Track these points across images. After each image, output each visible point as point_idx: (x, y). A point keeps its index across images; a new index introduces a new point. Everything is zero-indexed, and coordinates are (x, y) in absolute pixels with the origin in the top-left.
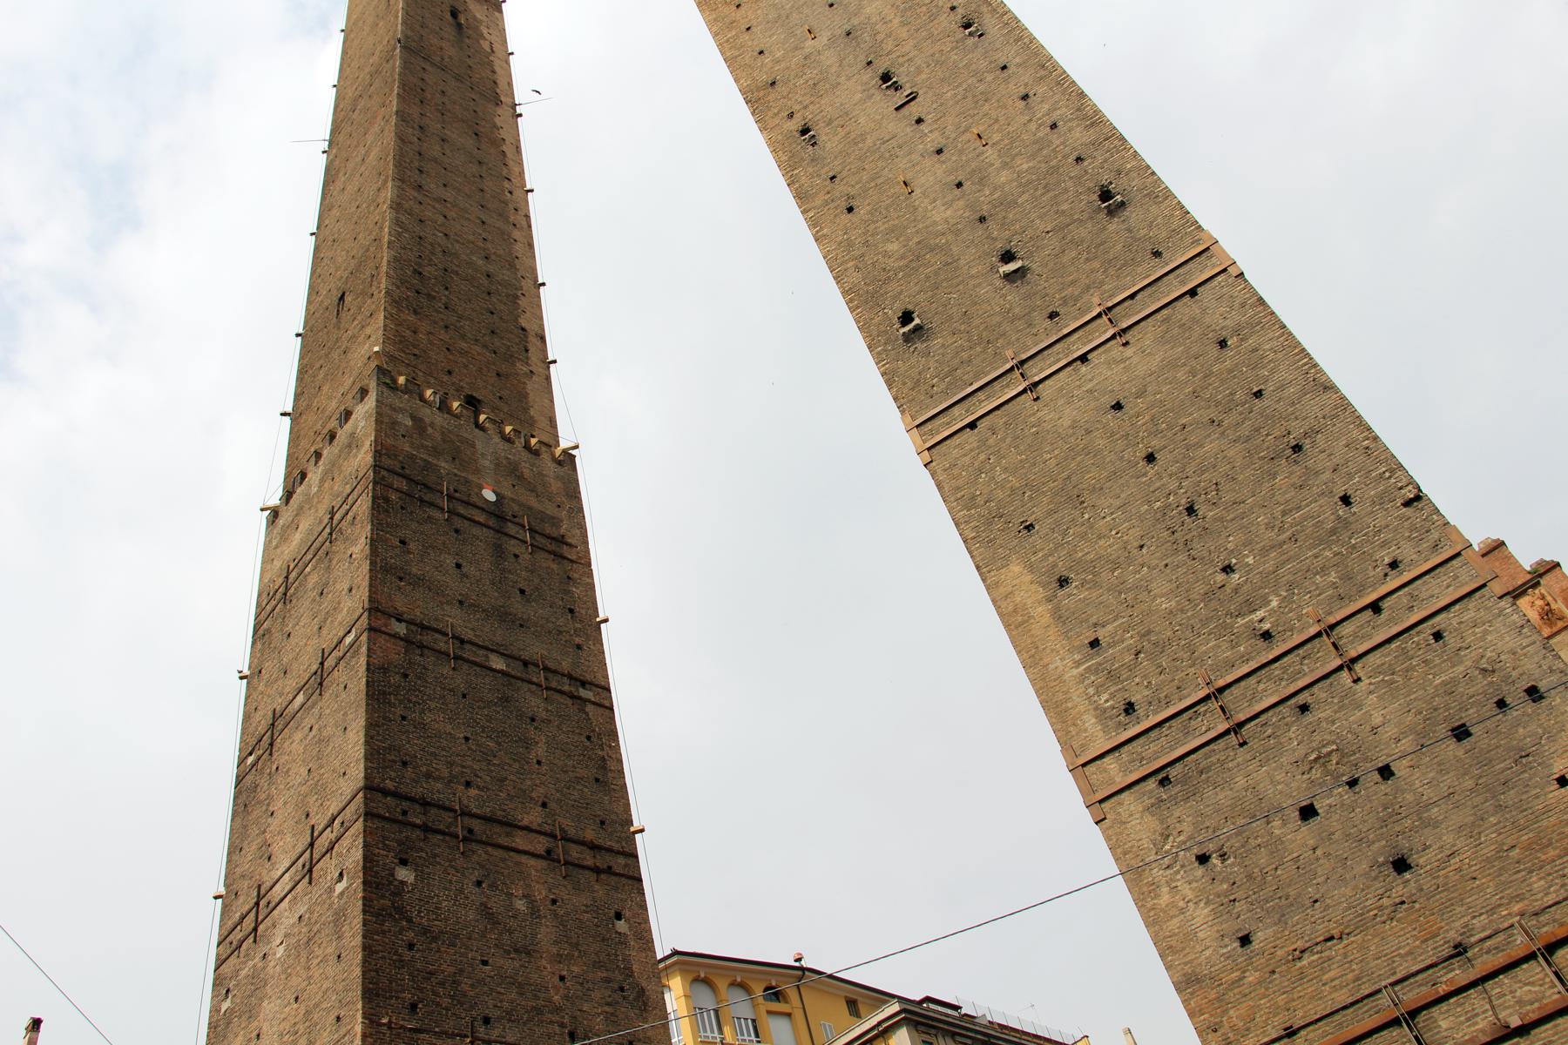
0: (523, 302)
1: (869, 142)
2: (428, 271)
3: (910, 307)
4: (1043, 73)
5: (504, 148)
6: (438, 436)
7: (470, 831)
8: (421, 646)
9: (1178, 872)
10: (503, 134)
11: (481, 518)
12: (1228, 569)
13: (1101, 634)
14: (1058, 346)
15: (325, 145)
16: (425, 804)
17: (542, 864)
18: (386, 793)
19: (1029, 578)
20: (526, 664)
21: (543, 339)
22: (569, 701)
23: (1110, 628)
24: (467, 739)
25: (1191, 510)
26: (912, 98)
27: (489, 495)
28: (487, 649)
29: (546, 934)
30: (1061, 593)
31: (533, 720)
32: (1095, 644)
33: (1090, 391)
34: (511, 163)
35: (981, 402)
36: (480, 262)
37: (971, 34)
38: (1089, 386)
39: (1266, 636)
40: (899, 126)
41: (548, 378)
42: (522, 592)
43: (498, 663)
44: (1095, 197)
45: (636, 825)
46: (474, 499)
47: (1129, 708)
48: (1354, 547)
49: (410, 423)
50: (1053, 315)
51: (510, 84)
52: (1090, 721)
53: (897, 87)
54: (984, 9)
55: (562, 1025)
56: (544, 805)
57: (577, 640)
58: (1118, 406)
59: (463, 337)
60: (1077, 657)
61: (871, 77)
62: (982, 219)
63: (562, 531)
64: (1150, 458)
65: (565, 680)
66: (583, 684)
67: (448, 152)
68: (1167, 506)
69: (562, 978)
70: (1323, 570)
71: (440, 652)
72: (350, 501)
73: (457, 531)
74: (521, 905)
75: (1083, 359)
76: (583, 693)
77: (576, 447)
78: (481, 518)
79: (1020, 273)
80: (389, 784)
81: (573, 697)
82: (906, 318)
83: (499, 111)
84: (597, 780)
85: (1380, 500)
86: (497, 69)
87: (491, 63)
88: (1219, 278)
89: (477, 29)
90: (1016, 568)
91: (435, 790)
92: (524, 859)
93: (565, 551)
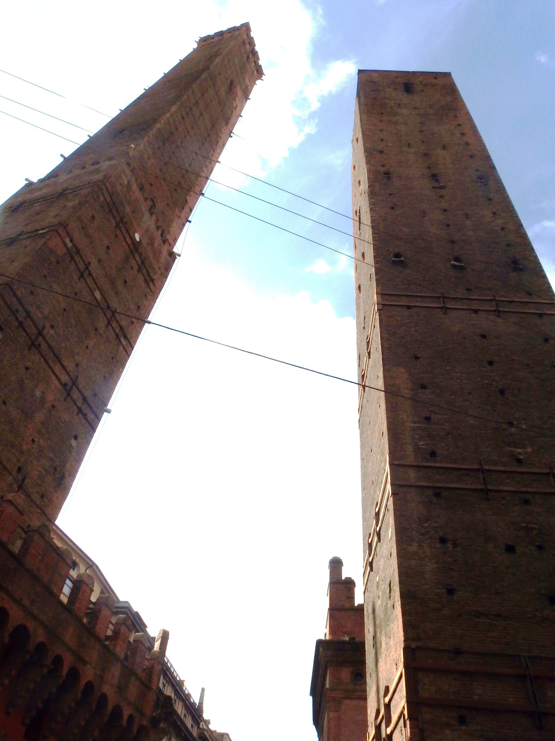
1: (414, 191)
3: (402, 253)
6: (133, 198)
7: (39, 345)
8: (72, 258)
9: (427, 539)
11: (129, 242)
12: (511, 424)
13: (434, 417)
15: (147, 88)
16: (28, 315)
17: (59, 386)
18: (15, 295)
19: (407, 376)
20: (108, 307)
21: (191, 210)
22: (115, 337)
23: (439, 417)
24: (65, 310)
25: (502, 392)
26: (443, 187)
27: (137, 237)
28: (97, 286)
29: (40, 416)
30: (420, 390)
31: (96, 330)
32: (428, 419)
34: (218, 147)
35: (417, 301)
37: (480, 182)
38: (474, 322)
39: (519, 461)
41: (184, 225)
42: (125, 282)
43: (98, 295)
45: (109, 407)
46: (131, 233)
47: (433, 454)
49: (126, 183)
50: (468, 290)
51: (234, 124)
52: (409, 449)
53: (437, 181)
54: (492, 178)
55: (18, 461)
56: (77, 365)
58: (483, 336)
60: (416, 419)
62: (453, 242)
63: (154, 277)
65: (119, 328)
66: (125, 337)
69: (33, 441)
71: (78, 268)
72: (79, 188)
73: (116, 236)
74: (38, 393)
75: (476, 311)
76: (122, 339)
77: (179, 255)
79: (461, 268)
80: (19, 293)
81: (117, 335)
82: (397, 255)
83: (226, 128)
87: (232, 112)
91: (37, 315)
92: (54, 377)
93: (151, 285)
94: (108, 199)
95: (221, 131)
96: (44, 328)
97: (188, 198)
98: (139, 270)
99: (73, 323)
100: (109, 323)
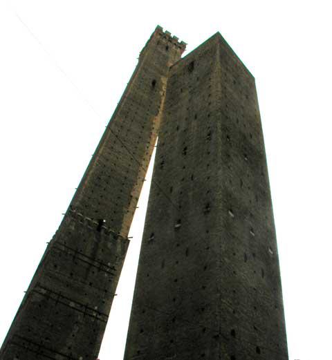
0: (135, 187)
2: (102, 177)
11: (86, 259)
16: (30, 341)
20: (82, 306)
34: (152, 136)
36: (125, 173)
41: (133, 213)
43: (72, 304)
57: (104, 300)
76: (98, 317)
78: (86, 259)
83: (156, 117)
84: (91, 343)
89: (162, 87)
93: (113, 272)
94: (63, 248)
95: (152, 124)
96: (42, 342)
97: (132, 194)
98: (99, 269)
99: (60, 328)
100: (85, 314)
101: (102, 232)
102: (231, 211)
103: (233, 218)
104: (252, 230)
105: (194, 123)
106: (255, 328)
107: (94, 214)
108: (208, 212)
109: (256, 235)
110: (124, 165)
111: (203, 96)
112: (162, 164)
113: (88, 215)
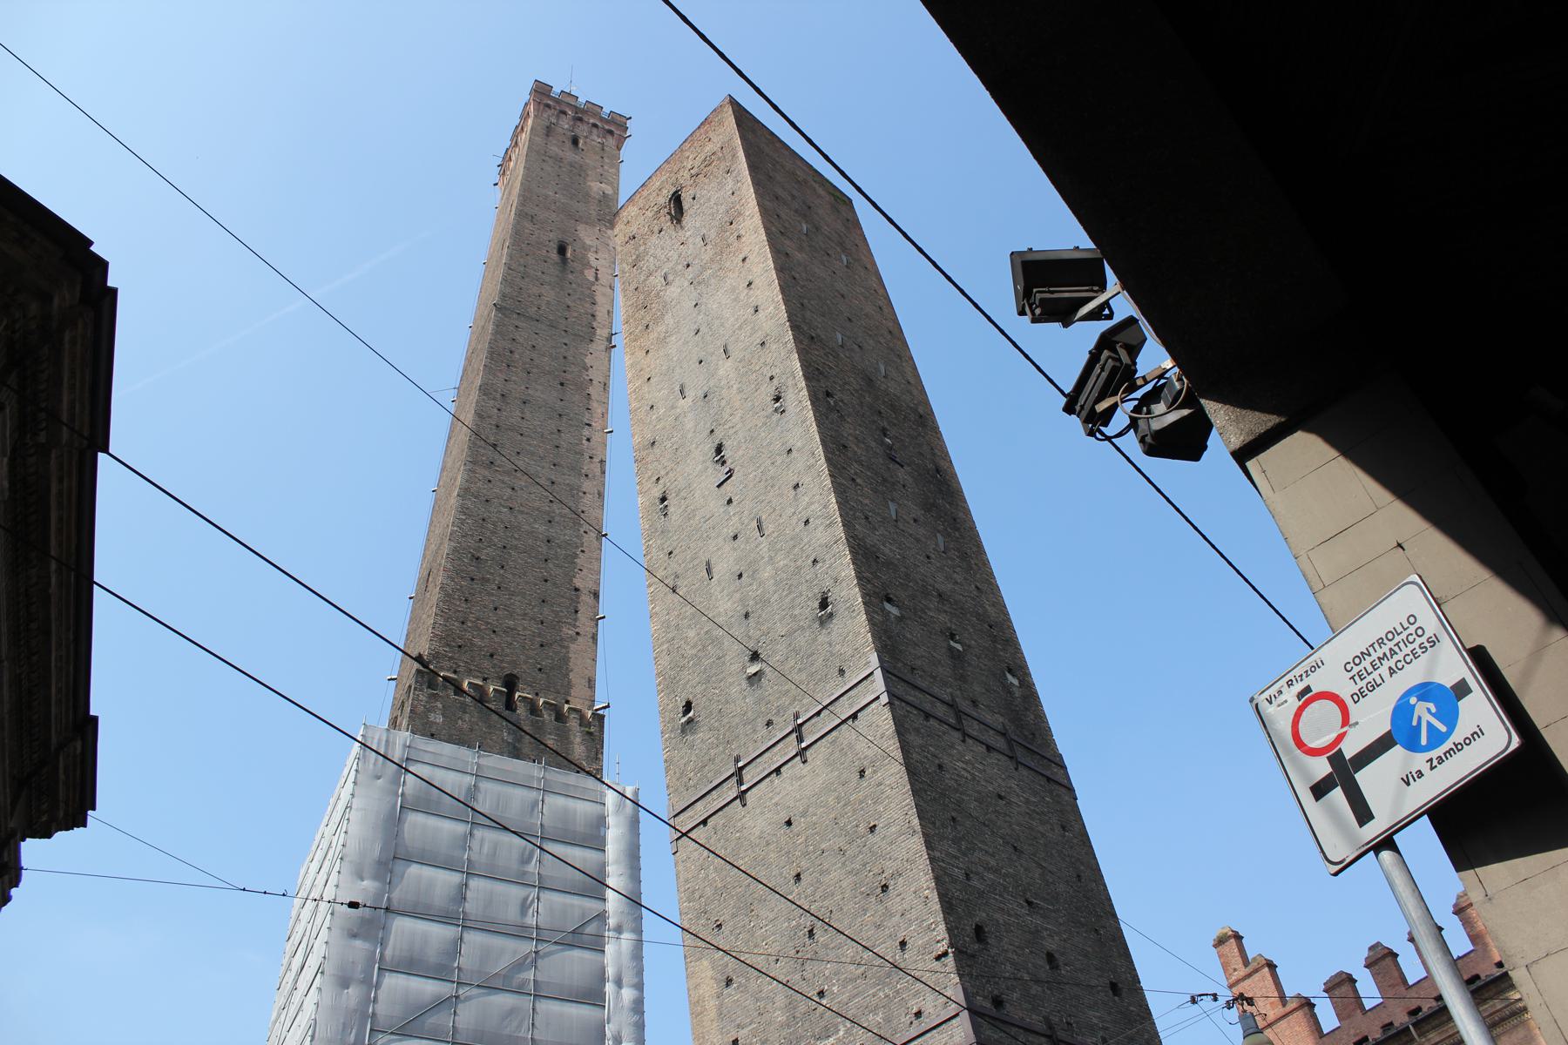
4: (812, 461)
5: (591, 390)
10: (592, 374)
14: (766, 755)
23: (746, 1031)
33: (776, 804)
34: (594, 405)
40: (715, 505)
41: (594, 638)
44: (816, 604)
48: (897, 992)
49: (440, 719)
58: (789, 823)
59: (511, 616)
61: (709, 448)
64: (798, 877)
67: (528, 415)
68: (799, 925)
70: (875, 1011)
85: (923, 950)
86: (599, 298)
88: (873, 706)
89: (584, 257)
90: (705, 963)
97: (578, 583)
101: (522, 711)
102: (889, 600)
103: (900, 619)
104: (952, 636)
105: (726, 368)
106: (1029, 903)
107: (486, 664)
108: (831, 615)
109: (967, 647)
110: (537, 504)
111: (733, 289)
112: (663, 499)
113: (469, 672)
